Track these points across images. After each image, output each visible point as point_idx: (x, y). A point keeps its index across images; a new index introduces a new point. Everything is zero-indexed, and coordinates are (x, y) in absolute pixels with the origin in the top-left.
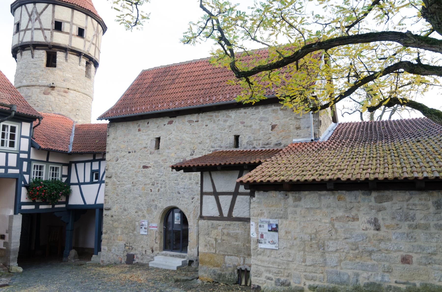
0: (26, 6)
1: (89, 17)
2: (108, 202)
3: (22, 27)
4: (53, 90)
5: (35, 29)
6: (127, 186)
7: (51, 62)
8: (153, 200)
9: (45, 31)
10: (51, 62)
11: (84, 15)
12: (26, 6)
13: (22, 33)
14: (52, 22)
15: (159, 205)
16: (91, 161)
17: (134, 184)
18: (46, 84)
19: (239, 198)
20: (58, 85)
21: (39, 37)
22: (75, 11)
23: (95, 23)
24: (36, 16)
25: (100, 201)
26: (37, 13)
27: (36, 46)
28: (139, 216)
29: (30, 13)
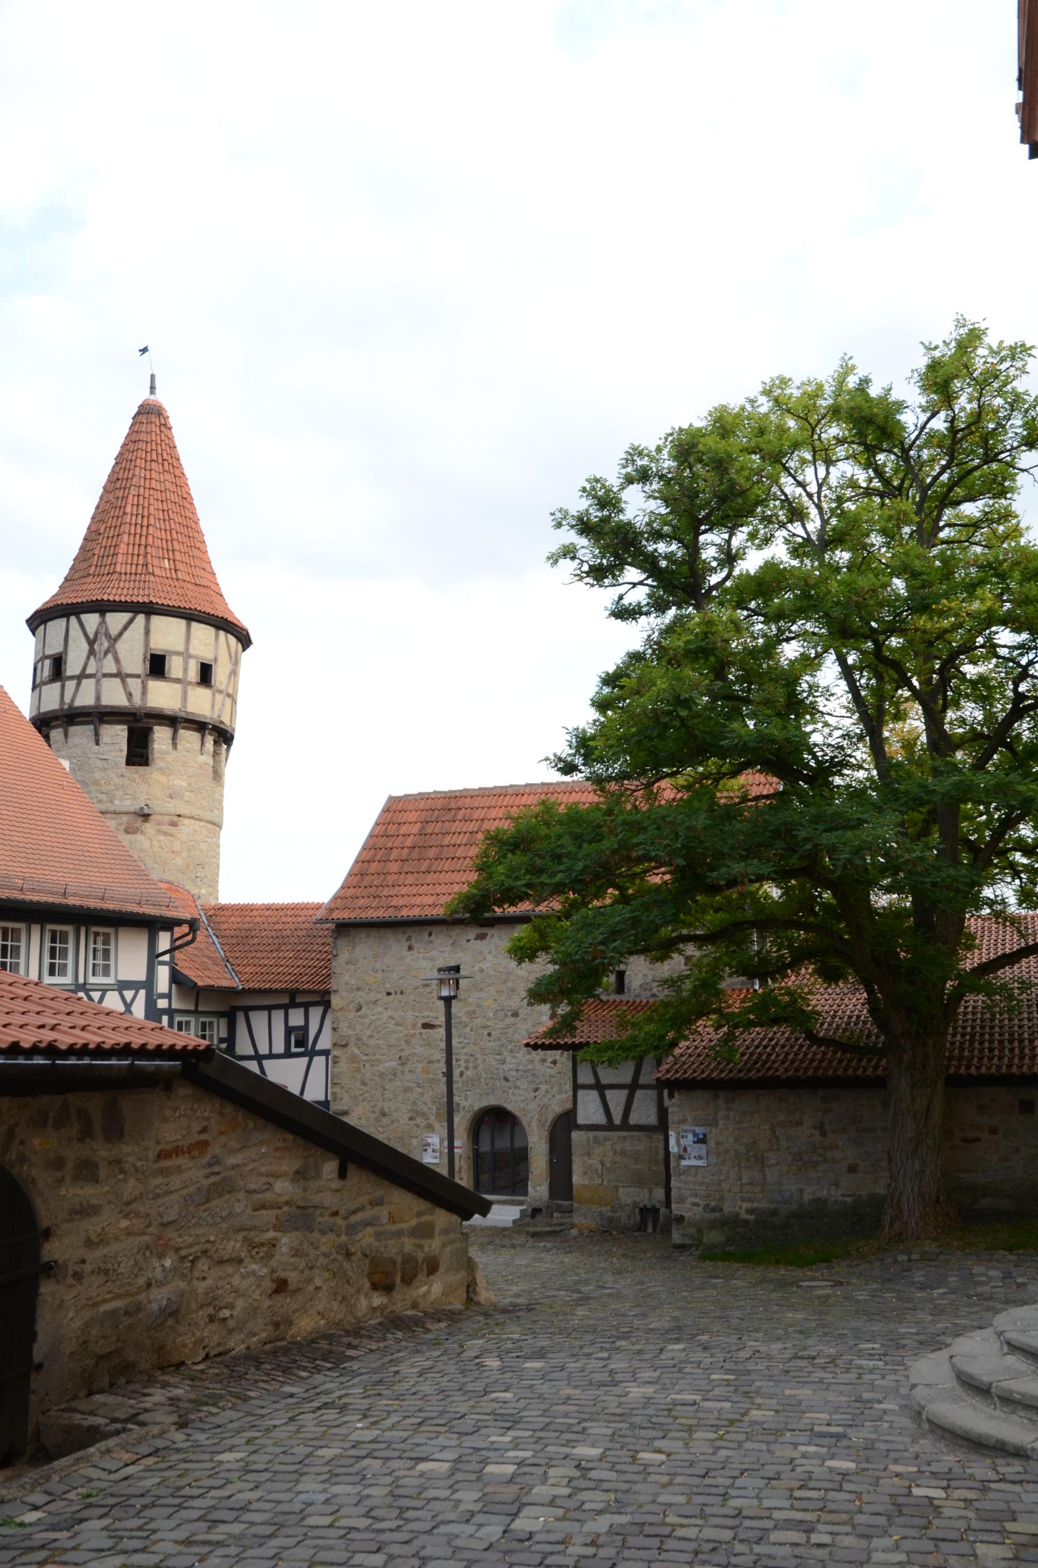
1: (222, 633)
3: (73, 667)
5: (105, 675)
6: (387, 1065)
7: (139, 753)
9: (129, 680)
10: (139, 753)
11: (212, 630)
16: (286, 1008)
17: (403, 1061)
18: (132, 809)
19: (639, 1094)
20: (158, 809)
21: (114, 696)
22: (194, 624)
23: (233, 640)
24: (106, 645)
26: (107, 635)
27: (100, 716)
29: (91, 636)
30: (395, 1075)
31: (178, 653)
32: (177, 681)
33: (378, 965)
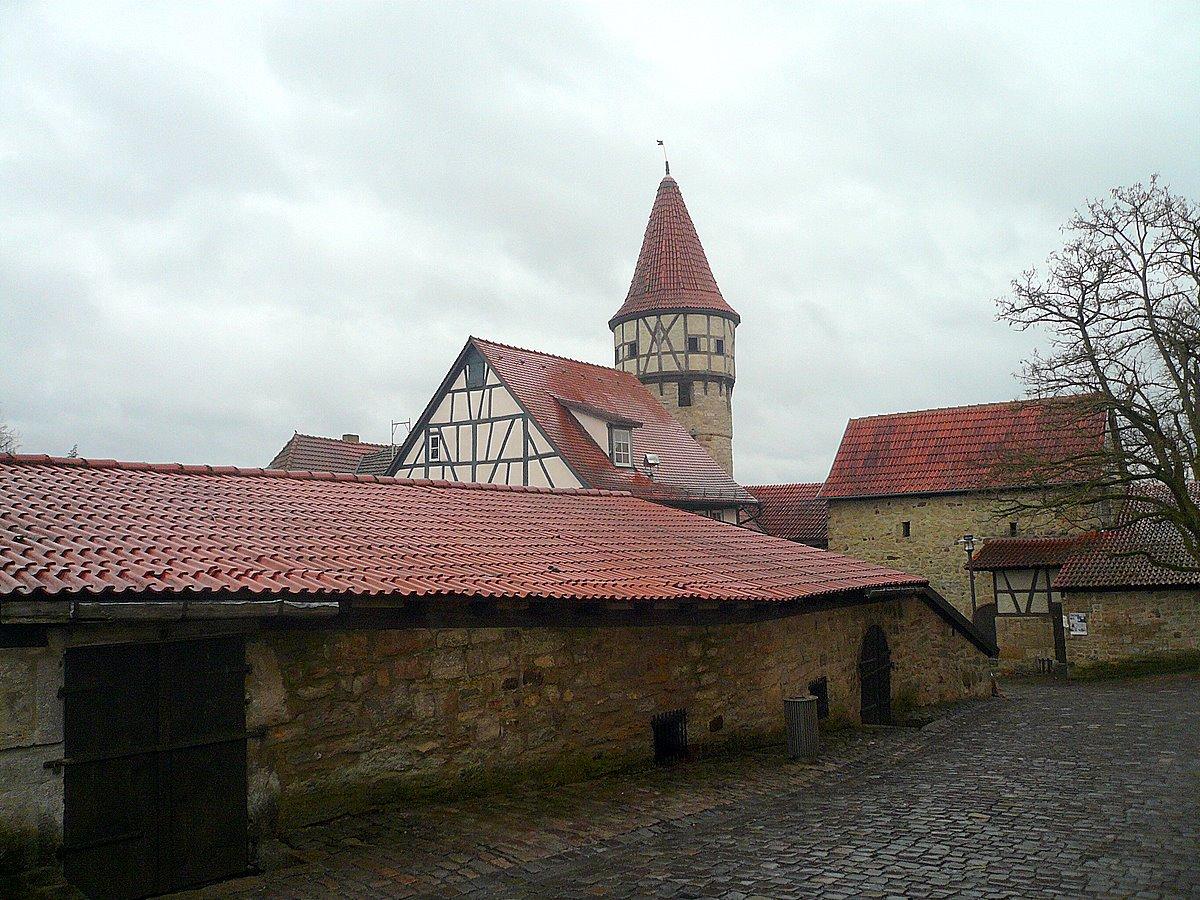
0: (645, 320)
3: (643, 349)
7: (685, 400)
10: (685, 400)
12: (645, 320)
21: (669, 365)
26: (662, 328)
27: (662, 378)
31: (704, 336)
32: (705, 353)
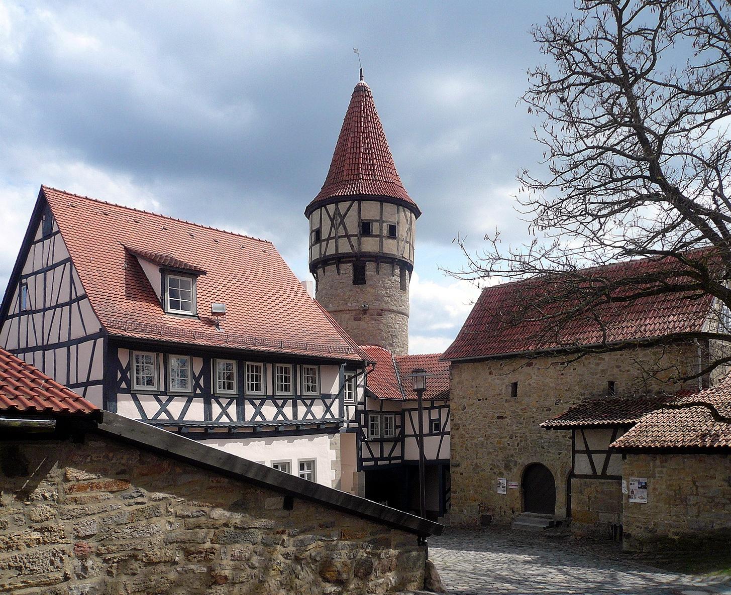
0: (326, 208)
2: (456, 458)
3: (324, 236)
4: (364, 314)
5: (339, 237)
7: (359, 278)
8: (512, 456)
10: (359, 278)
12: (326, 208)
13: (324, 244)
14: (359, 225)
15: (520, 461)
16: (429, 409)
17: (487, 437)
21: (345, 247)
25: (445, 455)
27: (338, 259)
28: (495, 473)
30: (483, 445)
31: (377, 221)
32: (377, 236)
33: (473, 384)
